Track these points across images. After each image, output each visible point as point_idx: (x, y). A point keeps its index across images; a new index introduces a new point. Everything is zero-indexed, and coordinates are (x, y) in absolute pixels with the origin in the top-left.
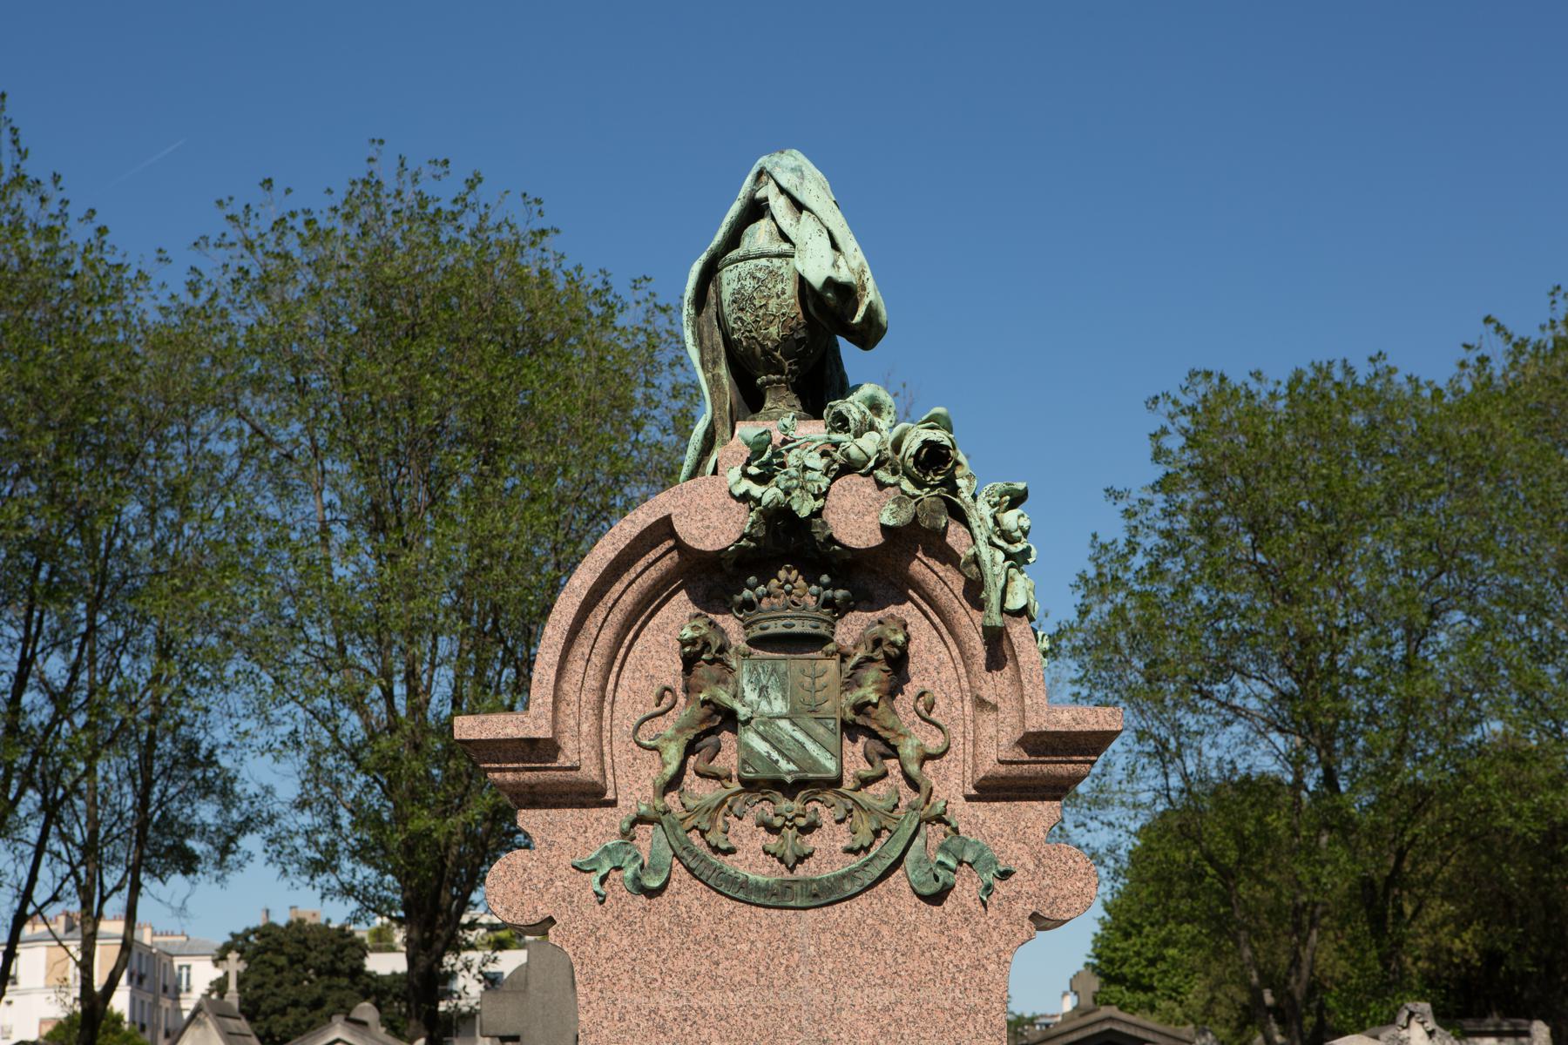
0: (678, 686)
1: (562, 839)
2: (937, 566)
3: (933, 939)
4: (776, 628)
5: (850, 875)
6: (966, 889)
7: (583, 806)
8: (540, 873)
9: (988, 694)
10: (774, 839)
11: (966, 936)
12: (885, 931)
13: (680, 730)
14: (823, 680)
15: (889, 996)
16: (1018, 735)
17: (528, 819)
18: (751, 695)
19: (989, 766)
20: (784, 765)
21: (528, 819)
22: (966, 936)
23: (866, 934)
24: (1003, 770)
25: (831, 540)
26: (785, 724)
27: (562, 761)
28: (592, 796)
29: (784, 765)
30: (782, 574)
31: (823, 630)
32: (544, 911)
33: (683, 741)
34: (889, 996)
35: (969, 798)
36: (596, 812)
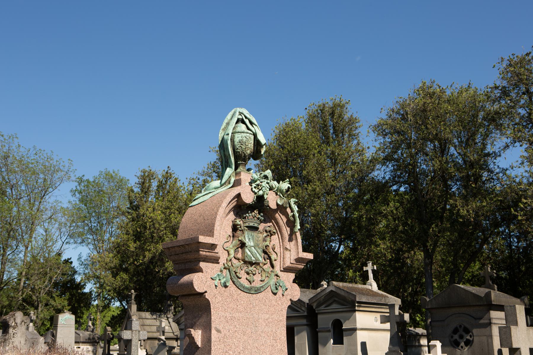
0: (231, 235)
1: (209, 271)
2: (281, 216)
3: (275, 303)
4: (251, 224)
5: (262, 287)
6: (280, 292)
7: (213, 263)
8: (204, 279)
9: (288, 247)
10: (248, 276)
11: (280, 303)
12: (267, 300)
13: (233, 247)
14: (259, 239)
15: (267, 316)
16: (296, 257)
17: (202, 265)
18: (247, 240)
19: (288, 264)
20: (253, 259)
21: (202, 265)
22: (280, 303)
23: (264, 301)
24: (290, 265)
25: (268, 206)
26: (253, 248)
27: (216, 251)
28: (216, 260)
29: (253, 259)
30: (255, 211)
31: (256, 225)
32: (205, 290)
33: (234, 249)
34: (267, 316)
35: (281, 271)
36: (215, 265)
